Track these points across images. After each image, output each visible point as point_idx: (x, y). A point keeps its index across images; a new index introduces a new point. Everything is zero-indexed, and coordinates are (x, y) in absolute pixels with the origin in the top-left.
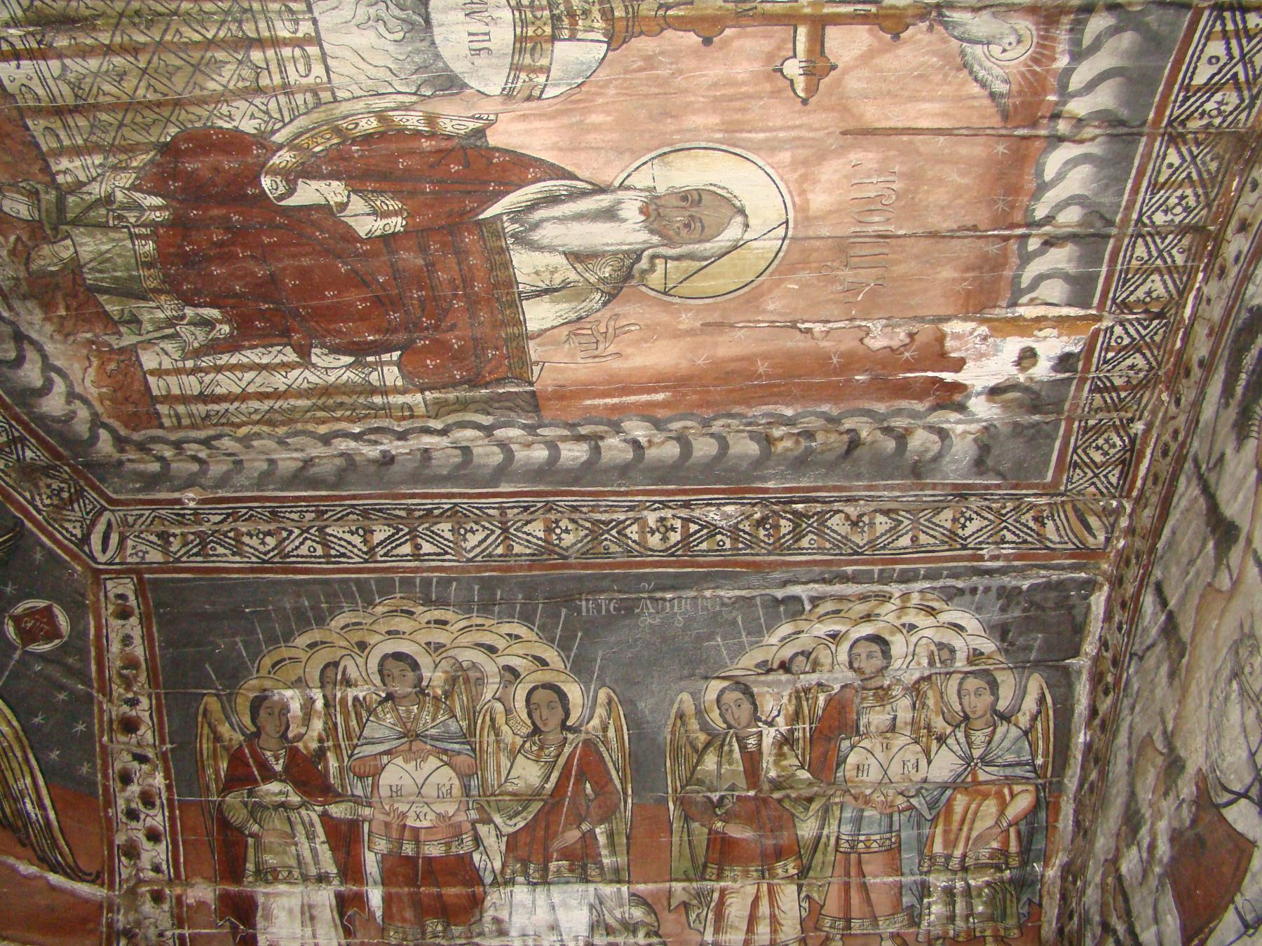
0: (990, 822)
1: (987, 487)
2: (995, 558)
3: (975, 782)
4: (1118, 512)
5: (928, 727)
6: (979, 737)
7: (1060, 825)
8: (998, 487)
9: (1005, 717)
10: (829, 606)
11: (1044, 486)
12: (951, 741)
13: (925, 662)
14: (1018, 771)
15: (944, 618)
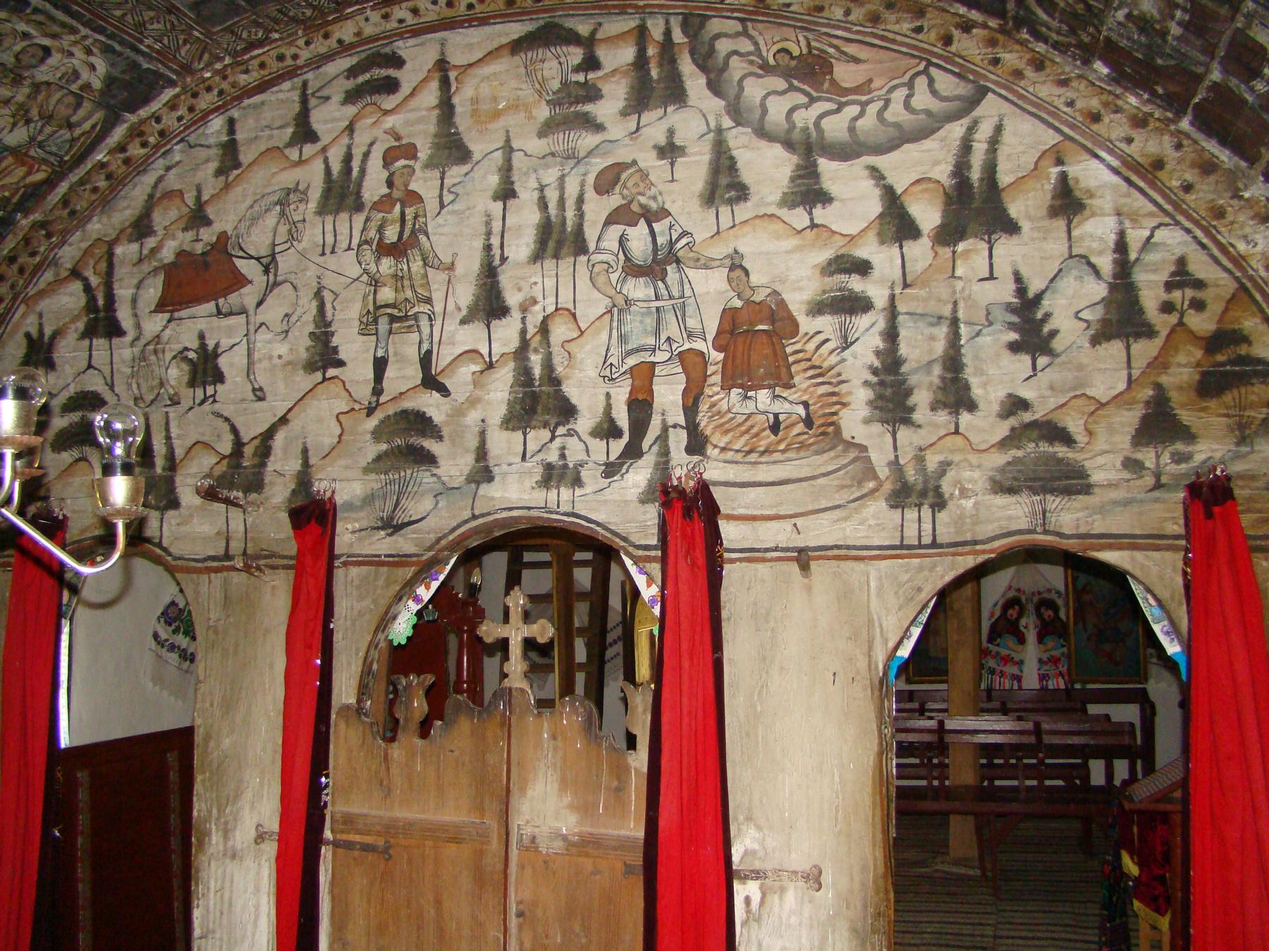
0: (14, 180)
1: (185, 15)
2: (148, 46)
3: (26, 154)
4: (221, 59)
5: (27, 112)
6: (48, 130)
7: (49, 198)
8: (190, 18)
9: (70, 126)
10: (40, 18)
11: (209, 31)
12: (32, 125)
13: (59, 75)
14: (52, 159)
15: (92, 59)
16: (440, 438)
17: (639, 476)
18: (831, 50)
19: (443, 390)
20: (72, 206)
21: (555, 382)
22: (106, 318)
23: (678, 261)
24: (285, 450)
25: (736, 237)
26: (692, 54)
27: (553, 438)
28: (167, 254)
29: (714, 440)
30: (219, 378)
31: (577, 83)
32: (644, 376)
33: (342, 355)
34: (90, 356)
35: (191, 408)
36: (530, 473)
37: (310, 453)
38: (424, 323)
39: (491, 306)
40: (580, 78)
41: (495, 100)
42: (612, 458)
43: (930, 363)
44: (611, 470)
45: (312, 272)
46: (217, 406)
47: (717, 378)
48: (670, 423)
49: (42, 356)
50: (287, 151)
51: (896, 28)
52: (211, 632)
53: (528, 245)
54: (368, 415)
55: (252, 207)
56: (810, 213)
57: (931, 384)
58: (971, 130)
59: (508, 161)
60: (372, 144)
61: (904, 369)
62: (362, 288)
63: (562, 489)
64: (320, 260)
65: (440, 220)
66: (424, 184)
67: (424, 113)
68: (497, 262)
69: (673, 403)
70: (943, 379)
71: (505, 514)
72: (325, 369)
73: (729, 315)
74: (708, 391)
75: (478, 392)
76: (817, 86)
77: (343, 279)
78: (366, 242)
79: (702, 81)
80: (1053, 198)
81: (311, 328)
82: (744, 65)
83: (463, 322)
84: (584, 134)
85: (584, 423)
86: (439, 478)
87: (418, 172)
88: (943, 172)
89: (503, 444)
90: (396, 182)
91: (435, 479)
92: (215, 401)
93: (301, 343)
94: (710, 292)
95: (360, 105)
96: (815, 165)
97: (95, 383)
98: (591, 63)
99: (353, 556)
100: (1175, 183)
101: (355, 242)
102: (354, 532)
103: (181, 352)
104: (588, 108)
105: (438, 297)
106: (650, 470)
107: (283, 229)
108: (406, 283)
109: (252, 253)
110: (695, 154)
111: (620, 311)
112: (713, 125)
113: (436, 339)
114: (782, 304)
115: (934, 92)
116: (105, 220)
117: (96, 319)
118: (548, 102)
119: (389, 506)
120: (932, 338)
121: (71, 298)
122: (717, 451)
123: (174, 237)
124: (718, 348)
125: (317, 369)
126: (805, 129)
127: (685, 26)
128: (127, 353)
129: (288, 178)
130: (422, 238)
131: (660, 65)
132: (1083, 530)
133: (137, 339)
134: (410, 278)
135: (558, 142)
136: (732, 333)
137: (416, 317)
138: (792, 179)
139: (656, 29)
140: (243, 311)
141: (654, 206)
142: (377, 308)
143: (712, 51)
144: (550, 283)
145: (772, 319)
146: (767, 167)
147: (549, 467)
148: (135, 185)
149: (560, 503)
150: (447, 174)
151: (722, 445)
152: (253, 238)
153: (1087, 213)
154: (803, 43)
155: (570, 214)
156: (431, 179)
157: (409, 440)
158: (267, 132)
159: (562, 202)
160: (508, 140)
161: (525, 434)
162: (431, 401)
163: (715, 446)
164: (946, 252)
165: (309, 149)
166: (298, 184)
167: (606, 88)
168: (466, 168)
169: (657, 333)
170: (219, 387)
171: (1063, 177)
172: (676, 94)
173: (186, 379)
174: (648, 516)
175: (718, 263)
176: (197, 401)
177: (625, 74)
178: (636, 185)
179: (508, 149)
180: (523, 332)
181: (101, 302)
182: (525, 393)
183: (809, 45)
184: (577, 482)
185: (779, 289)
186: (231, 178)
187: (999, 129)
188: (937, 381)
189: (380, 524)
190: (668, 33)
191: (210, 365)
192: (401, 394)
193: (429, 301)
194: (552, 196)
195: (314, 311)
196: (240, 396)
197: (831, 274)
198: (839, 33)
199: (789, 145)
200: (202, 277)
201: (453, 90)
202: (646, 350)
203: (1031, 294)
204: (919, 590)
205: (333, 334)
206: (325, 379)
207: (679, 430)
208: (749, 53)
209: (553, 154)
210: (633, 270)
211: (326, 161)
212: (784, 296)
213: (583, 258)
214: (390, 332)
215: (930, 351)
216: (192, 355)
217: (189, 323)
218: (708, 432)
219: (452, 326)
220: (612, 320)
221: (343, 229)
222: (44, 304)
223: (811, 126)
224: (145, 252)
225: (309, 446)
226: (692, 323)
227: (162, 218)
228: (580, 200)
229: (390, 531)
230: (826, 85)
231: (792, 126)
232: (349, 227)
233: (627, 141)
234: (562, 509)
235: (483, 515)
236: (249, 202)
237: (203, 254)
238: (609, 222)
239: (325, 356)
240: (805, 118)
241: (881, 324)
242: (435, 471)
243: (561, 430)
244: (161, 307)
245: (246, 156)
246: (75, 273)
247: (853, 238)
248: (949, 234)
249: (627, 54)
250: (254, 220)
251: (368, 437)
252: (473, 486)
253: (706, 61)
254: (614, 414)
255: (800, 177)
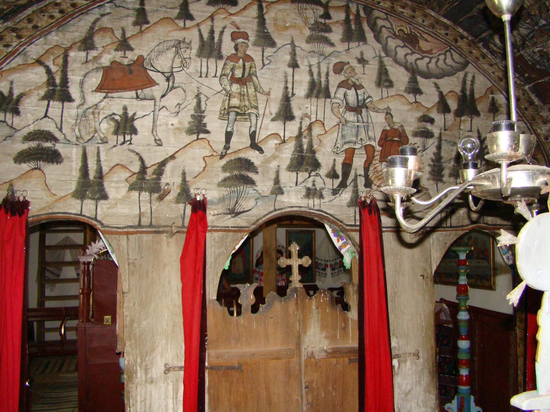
16: (257, 173)
17: (346, 196)
18: (418, 35)
19: (261, 150)
20: (34, 23)
21: (314, 152)
22: (61, 90)
23: (367, 108)
24: (172, 172)
25: (388, 101)
26: (368, 23)
27: (310, 176)
28: (106, 60)
29: (375, 182)
30: (134, 131)
31: (321, 23)
32: (350, 153)
33: (208, 128)
34: (47, 110)
35: (115, 146)
36: (300, 191)
37: (187, 175)
38: (253, 118)
39: (286, 114)
40: (323, 21)
41: (285, 21)
42: (335, 187)
43: (450, 160)
44: (335, 192)
45: (195, 85)
46: (131, 147)
47: (378, 158)
48: (358, 174)
49: (11, 106)
50: (176, 21)
51: (440, 31)
52: (131, 266)
53: (304, 90)
54: (221, 158)
55: (158, 45)
56: (415, 97)
57: (450, 167)
58: (465, 76)
59: (294, 50)
60: (224, 28)
61: (442, 161)
62: (222, 97)
63: (315, 199)
64: (200, 80)
65: (263, 71)
66: (254, 52)
67: (250, 19)
68: (290, 95)
69: (360, 166)
70: (454, 166)
71: (289, 209)
72: (198, 133)
73: (384, 132)
74: (374, 162)
75: (277, 153)
76: (414, 47)
77: (212, 91)
78: (224, 75)
79: (372, 35)
80: (490, 105)
81: (193, 112)
82: (387, 32)
83: (273, 120)
84: (326, 46)
85: (323, 171)
86: (257, 191)
87: (250, 46)
88: (458, 90)
89: (287, 178)
90: (239, 49)
91: (255, 192)
92: (131, 144)
93: (186, 118)
94: (378, 121)
95: (217, 8)
96: (416, 79)
97: (49, 126)
98: (327, 16)
99: (214, 227)
100: (523, 107)
101: (219, 74)
102: (214, 215)
103: (110, 116)
104: (326, 35)
105: (261, 107)
106: (351, 193)
107: (178, 61)
108: (246, 98)
109: (160, 69)
110: (372, 65)
111: (343, 125)
112: (378, 54)
113: (258, 126)
114: (404, 130)
115: (453, 59)
116: (61, 35)
117: (54, 91)
118: (309, 28)
119: (233, 203)
120: (452, 150)
121: (38, 76)
122: (376, 187)
123: (109, 53)
124: (380, 145)
125: (194, 133)
126: (411, 63)
127: (365, 9)
128: (74, 112)
129: (179, 35)
130: (254, 78)
131: (355, 24)
132: (494, 223)
133: (82, 104)
134: (248, 96)
135: (315, 46)
136: (385, 140)
137: (249, 114)
138: (409, 82)
139: (353, 8)
140: (153, 99)
141: (358, 83)
142: (230, 107)
143: (375, 24)
144: (314, 108)
145: (400, 137)
146: (399, 76)
147: (308, 189)
148: (80, 20)
149: (312, 205)
150: (265, 51)
151: (378, 184)
152: (160, 62)
153: (499, 113)
154: (408, 29)
155: (323, 79)
156: (257, 51)
157: (241, 173)
158: (164, 9)
159: (319, 74)
160: (293, 41)
161: (297, 174)
162: (254, 155)
163: (375, 185)
164: (458, 119)
165: (189, 23)
166: (184, 39)
167: (334, 28)
168: (274, 50)
169: (357, 136)
170: (134, 136)
171: (493, 98)
172: (362, 38)
173: (112, 130)
174: (351, 212)
175: (381, 111)
176: (119, 143)
177: (342, 24)
178: (350, 73)
179: (292, 44)
180: (300, 128)
181: (58, 81)
182: (299, 156)
183: (410, 31)
184: (321, 196)
185: (403, 124)
186: (143, 28)
187: (474, 77)
188: (452, 167)
189: (228, 212)
190: (358, 11)
191: (128, 125)
192: (239, 150)
193: (256, 108)
194: (315, 70)
195: (195, 104)
196: (146, 143)
197: (421, 122)
198: (421, 28)
199: (407, 69)
200: (127, 77)
201: (265, 11)
202: (352, 143)
203: (482, 138)
204: (446, 243)
205: (204, 117)
206: (198, 139)
207: (361, 177)
208: (389, 28)
209: (314, 52)
210: (348, 108)
211: (200, 31)
212: (405, 128)
213: (328, 100)
214: (235, 120)
215: (451, 155)
216: (117, 118)
217: (118, 101)
218: (372, 179)
219: (267, 121)
220: (339, 128)
221: (212, 67)
222: (15, 77)
223: (413, 63)
224: (90, 58)
225: (186, 171)
226: (371, 134)
227: (98, 40)
228: (327, 75)
229: (233, 215)
230: (417, 48)
231: (407, 62)
232: (214, 66)
233: (344, 53)
234: (315, 208)
235: (279, 209)
236: (157, 42)
237: (128, 65)
238: (339, 86)
239: (198, 127)
240: (411, 59)
241: (436, 143)
242: (255, 188)
243: (313, 173)
244: (100, 89)
245: (153, 19)
246: (39, 62)
247: (429, 109)
248: (459, 113)
249: (342, 16)
250: (160, 53)
251: (220, 169)
252: (274, 196)
253: (373, 27)
254: (336, 168)
255: (411, 82)
